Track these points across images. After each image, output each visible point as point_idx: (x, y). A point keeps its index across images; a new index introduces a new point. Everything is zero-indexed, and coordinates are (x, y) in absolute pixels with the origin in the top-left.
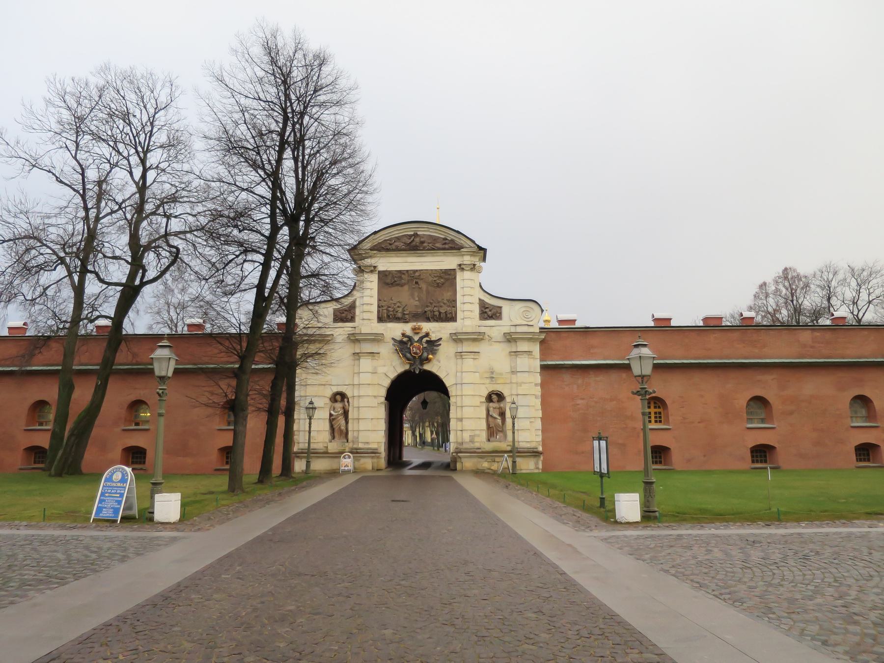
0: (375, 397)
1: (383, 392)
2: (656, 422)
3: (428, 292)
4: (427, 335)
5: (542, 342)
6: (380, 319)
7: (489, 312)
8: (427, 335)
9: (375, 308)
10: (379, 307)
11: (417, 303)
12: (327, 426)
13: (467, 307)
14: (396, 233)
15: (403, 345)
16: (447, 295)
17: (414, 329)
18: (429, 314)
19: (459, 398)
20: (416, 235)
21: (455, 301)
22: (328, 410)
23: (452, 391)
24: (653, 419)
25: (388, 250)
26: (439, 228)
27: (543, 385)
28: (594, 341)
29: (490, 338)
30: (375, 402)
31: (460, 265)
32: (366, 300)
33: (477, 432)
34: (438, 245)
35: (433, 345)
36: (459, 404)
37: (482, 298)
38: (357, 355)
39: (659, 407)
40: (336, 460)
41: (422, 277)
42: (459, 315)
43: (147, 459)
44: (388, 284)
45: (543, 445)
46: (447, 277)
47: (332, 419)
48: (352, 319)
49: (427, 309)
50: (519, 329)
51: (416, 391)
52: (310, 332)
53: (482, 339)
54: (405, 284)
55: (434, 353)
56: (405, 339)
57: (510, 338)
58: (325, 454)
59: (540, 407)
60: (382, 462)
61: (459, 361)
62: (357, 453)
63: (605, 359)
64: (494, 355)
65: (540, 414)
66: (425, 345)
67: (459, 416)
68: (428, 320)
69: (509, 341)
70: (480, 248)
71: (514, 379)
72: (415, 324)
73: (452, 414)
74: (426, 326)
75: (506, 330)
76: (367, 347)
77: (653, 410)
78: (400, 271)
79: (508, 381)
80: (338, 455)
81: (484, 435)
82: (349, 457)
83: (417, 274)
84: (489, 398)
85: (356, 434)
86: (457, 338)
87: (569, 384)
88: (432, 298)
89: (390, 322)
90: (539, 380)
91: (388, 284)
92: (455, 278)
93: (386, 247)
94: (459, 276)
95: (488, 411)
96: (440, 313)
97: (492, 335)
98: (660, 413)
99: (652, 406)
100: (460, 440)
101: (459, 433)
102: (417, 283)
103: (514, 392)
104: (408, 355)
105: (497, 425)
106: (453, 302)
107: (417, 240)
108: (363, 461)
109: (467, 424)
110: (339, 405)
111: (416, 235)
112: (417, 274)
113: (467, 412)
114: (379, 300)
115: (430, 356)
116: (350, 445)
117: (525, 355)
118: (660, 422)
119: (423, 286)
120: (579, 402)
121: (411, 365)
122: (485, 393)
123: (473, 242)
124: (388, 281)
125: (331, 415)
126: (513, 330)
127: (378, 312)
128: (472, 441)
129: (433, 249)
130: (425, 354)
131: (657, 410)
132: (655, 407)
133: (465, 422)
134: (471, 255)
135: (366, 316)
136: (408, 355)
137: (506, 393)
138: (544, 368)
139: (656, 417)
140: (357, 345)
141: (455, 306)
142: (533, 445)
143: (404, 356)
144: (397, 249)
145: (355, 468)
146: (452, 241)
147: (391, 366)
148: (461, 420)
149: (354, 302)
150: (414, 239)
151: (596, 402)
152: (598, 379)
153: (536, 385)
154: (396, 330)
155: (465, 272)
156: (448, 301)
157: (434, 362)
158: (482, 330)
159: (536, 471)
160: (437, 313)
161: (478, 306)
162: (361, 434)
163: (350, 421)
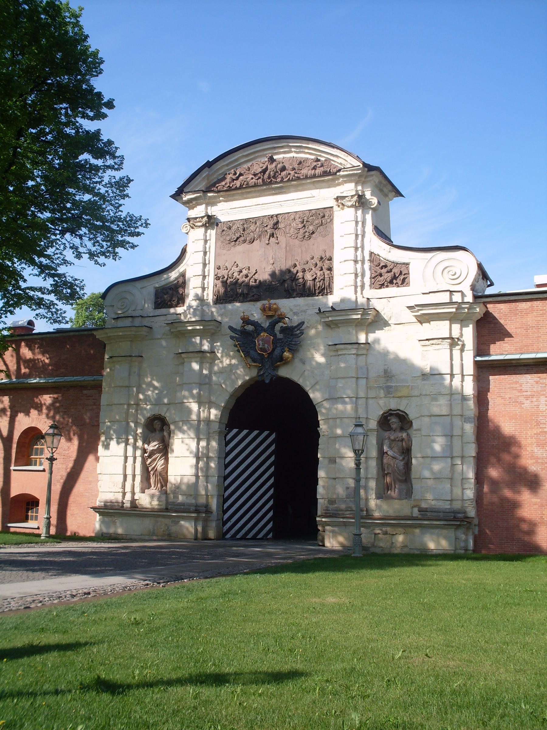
21: (330, 259)
31: (337, 199)
34: (304, 171)
41: (281, 226)
56: (250, 328)
66: (280, 336)
70: (369, 168)
102: (272, 235)
104: (252, 352)
115: (286, 354)
129: (298, 178)
138: (478, 366)
141: (330, 269)
142: (457, 505)
146: (327, 160)
155: (346, 209)
157: (297, 361)
161: (367, 265)
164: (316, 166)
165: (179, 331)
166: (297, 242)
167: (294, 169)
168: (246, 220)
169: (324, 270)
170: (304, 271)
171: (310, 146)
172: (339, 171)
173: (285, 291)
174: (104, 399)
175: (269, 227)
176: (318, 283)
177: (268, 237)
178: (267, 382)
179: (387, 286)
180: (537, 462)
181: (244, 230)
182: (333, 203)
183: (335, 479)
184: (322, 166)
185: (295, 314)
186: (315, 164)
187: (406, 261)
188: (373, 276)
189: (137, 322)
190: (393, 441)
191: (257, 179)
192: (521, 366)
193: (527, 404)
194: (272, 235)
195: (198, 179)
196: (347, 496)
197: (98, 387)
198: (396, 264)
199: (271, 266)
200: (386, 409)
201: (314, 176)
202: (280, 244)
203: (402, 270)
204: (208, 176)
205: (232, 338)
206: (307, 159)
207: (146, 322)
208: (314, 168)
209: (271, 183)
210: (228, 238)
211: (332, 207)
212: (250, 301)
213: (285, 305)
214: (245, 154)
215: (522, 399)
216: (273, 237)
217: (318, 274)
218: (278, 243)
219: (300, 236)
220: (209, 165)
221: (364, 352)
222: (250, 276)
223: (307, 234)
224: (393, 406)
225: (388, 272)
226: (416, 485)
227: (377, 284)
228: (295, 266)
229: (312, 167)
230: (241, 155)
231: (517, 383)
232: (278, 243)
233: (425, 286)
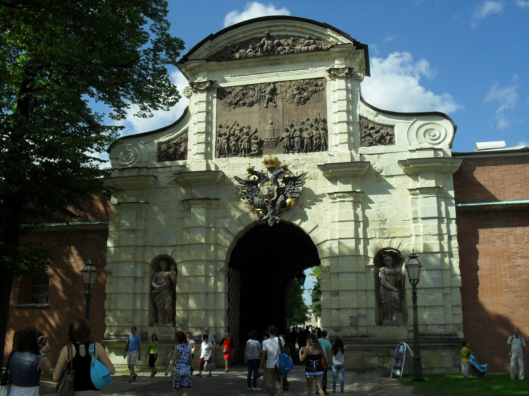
21: (325, 121)
22: (148, 280)
31: (329, 71)
33: (363, 312)
34: (298, 47)
37: (365, 115)
38: (187, 203)
41: (278, 91)
45: (465, 331)
67: (334, 286)
81: (372, 315)
101: (334, 312)
102: (270, 100)
120: (520, 262)
125: (152, 288)
128: (354, 324)
130: (281, 197)
141: (325, 130)
142: (450, 329)
148: (336, 293)
164: (309, 43)
165: (186, 180)
167: (288, 45)
168: (246, 87)
169: (320, 130)
170: (301, 131)
171: (304, 26)
173: (284, 147)
175: (267, 92)
176: (314, 141)
177: (266, 101)
179: (376, 145)
180: (511, 291)
181: (244, 95)
182: (326, 75)
183: (338, 309)
184: (314, 43)
186: (308, 41)
187: (392, 124)
188: (363, 135)
190: (388, 275)
191: (256, 52)
192: (491, 211)
193: (498, 243)
194: (270, 100)
195: (201, 49)
196: (350, 324)
198: (383, 126)
199: (270, 126)
201: (308, 51)
202: (278, 107)
203: (388, 131)
204: (210, 47)
207: (151, 173)
208: (308, 45)
209: (269, 55)
210: (229, 101)
213: (289, 160)
214: (244, 30)
215: (494, 239)
216: (271, 101)
217: (314, 133)
218: (276, 107)
219: (295, 100)
220: (212, 37)
223: (302, 99)
227: (366, 143)
228: (292, 126)
229: (305, 43)
230: (239, 31)
232: (276, 107)
233: (410, 144)
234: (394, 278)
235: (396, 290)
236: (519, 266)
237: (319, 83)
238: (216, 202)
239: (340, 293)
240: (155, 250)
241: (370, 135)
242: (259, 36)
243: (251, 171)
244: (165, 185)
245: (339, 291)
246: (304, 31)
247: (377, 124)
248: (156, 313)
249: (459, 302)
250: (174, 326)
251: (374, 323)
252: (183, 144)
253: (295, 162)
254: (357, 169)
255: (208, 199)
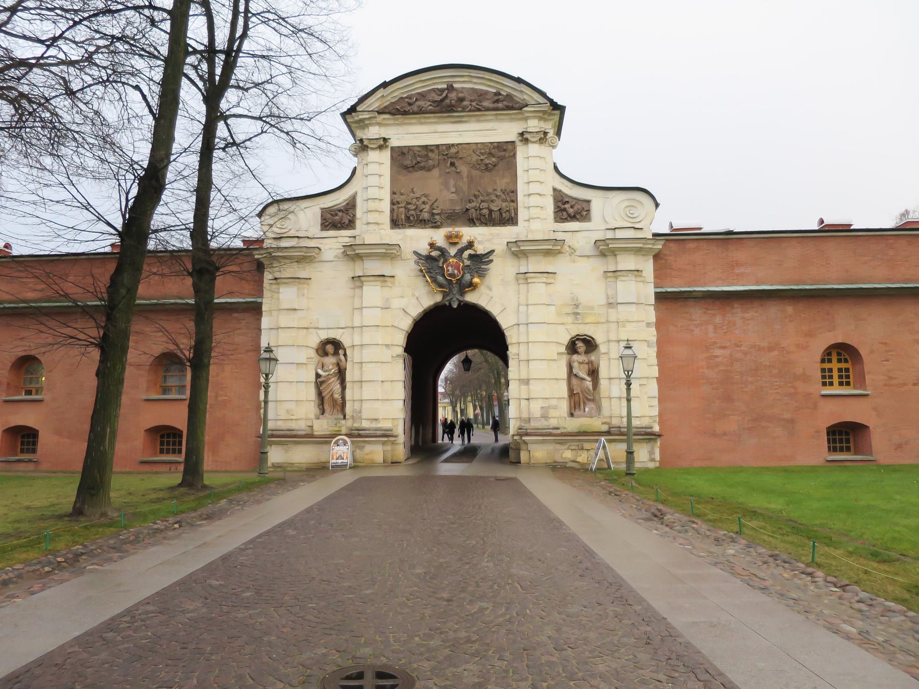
0: (387, 346)
1: (400, 339)
2: (841, 384)
3: (471, 179)
4: (470, 245)
5: (657, 257)
6: (395, 223)
7: (569, 209)
8: (470, 245)
9: (386, 206)
10: (392, 203)
11: (454, 197)
12: (311, 393)
13: (534, 200)
14: (417, 86)
15: (431, 263)
16: (502, 183)
17: (449, 237)
18: (473, 214)
19: (523, 348)
20: (450, 88)
21: (514, 192)
23: (511, 337)
24: (836, 380)
25: (405, 113)
26: (487, 75)
27: (660, 324)
28: (739, 254)
29: (573, 250)
30: (387, 355)
31: (522, 134)
32: (373, 193)
33: (554, 402)
34: (486, 104)
35: (480, 262)
36: (523, 357)
37: (559, 187)
38: (358, 280)
39: (846, 361)
40: (325, 447)
42: (522, 215)
43: (39, 447)
44: (406, 168)
45: (661, 423)
46: (503, 153)
47: (319, 382)
48: (351, 224)
49: (469, 206)
50: (620, 234)
51: (454, 335)
52: (284, 244)
53: (560, 252)
54: (434, 166)
55: (482, 274)
57: (605, 249)
58: (309, 437)
59: (655, 361)
60: (400, 451)
61: (523, 287)
62: (360, 436)
63: (758, 284)
64: (578, 278)
65: (656, 373)
66: (467, 263)
67: (524, 376)
68: (472, 222)
69: (603, 254)
71: (613, 315)
72: (450, 229)
73: (513, 372)
74: (468, 233)
75: (600, 236)
76: (374, 267)
77: (835, 365)
78: (426, 147)
79: (603, 320)
80: (326, 439)
81: (564, 406)
82: (345, 443)
83: (453, 150)
84: (572, 348)
85: (357, 406)
86: (518, 250)
87: (701, 323)
88: (480, 189)
89: (411, 227)
90: (653, 318)
91: (406, 168)
92: (514, 156)
93: (402, 110)
94: (521, 152)
95: (570, 367)
96: (491, 211)
97: (576, 245)
98: (847, 370)
99: (834, 358)
100: (525, 415)
101: (524, 403)
102: (452, 164)
103: (613, 337)
104: (440, 278)
105: (585, 391)
106: (511, 194)
107: (453, 95)
108: (368, 448)
109: (536, 389)
110: (330, 361)
111: (450, 88)
112: (453, 150)
113: (537, 369)
114: (393, 193)
116: (349, 423)
117: (631, 276)
118: (848, 384)
119: (463, 169)
120: (718, 352)
121: (445, 295)
122: (566, 340)
123: (543, 94)
124: (408, 162)
125: (318, 376)
126: (610, 235)
127: (392, 211)
128: (545, 417)
129: (479, 110)
130: (468, 277)
131: (843, 365)
132: (839, 361)
133: (534, 386)
134: (540, 119)
135: (372, 217)
136: (440, 278)
137: (599, 338)
139: (840, 377)
140: (358, 264)
141: (514, 201)
143: (435, 281)
144: (421, 112)
145: (354, 460)
146: (509, 96)
147: (413, 298)
148: (527, 382)
149: (353, 199)
150: (445, 92)
151: (745, 354)
152: (746, 315)
153: (648, 325)
154: (419, 239)
155: (530, 145)
156: (503, 192)
157: (482, 289)
158: (559, 236)
159: (651, 465)
160: (485, 212)
162: (366, 406)
163: (348, 385)
166: (478, 173)
172: (527, 106)
173: (469, 220)
174: (265, 322)
177: (449, 164)
178: (455, 306)
185: (480, 242)
189: (304, 243)
193: (697, 331)
197: (256, 310)
200: (574, 334)
205: (417, 263)
206: (487, 92)
211: (513, 142)
212: (432, 227)
220: (385, 85)
221: (552, 281)
222: (430, 203)
224: (580, 333)
225: (572, 207)
226: (605, 403)
231: (687, 313)
234: (586, 366)
235: (589, 379)
236: (716, 357)
237: (510, 147)
238: (392, 279)
239: (531, 382)
240: (321, 332)
241: (565, 210)
242: (440, 87)
243: (432, 245)
244: (332, 258)
245: (528, 380)
246: (492, 84)
247: (572, 198)
248: (322, 404)
249: (656, 394)
250: (345, 418)
251: (566, 415)
252: (351, 211)
253: (483, 237)
254: (550, 247)
255: (384, 276)
